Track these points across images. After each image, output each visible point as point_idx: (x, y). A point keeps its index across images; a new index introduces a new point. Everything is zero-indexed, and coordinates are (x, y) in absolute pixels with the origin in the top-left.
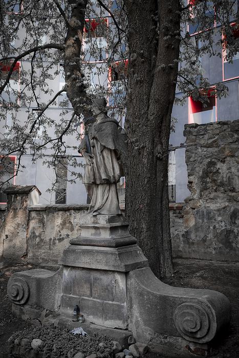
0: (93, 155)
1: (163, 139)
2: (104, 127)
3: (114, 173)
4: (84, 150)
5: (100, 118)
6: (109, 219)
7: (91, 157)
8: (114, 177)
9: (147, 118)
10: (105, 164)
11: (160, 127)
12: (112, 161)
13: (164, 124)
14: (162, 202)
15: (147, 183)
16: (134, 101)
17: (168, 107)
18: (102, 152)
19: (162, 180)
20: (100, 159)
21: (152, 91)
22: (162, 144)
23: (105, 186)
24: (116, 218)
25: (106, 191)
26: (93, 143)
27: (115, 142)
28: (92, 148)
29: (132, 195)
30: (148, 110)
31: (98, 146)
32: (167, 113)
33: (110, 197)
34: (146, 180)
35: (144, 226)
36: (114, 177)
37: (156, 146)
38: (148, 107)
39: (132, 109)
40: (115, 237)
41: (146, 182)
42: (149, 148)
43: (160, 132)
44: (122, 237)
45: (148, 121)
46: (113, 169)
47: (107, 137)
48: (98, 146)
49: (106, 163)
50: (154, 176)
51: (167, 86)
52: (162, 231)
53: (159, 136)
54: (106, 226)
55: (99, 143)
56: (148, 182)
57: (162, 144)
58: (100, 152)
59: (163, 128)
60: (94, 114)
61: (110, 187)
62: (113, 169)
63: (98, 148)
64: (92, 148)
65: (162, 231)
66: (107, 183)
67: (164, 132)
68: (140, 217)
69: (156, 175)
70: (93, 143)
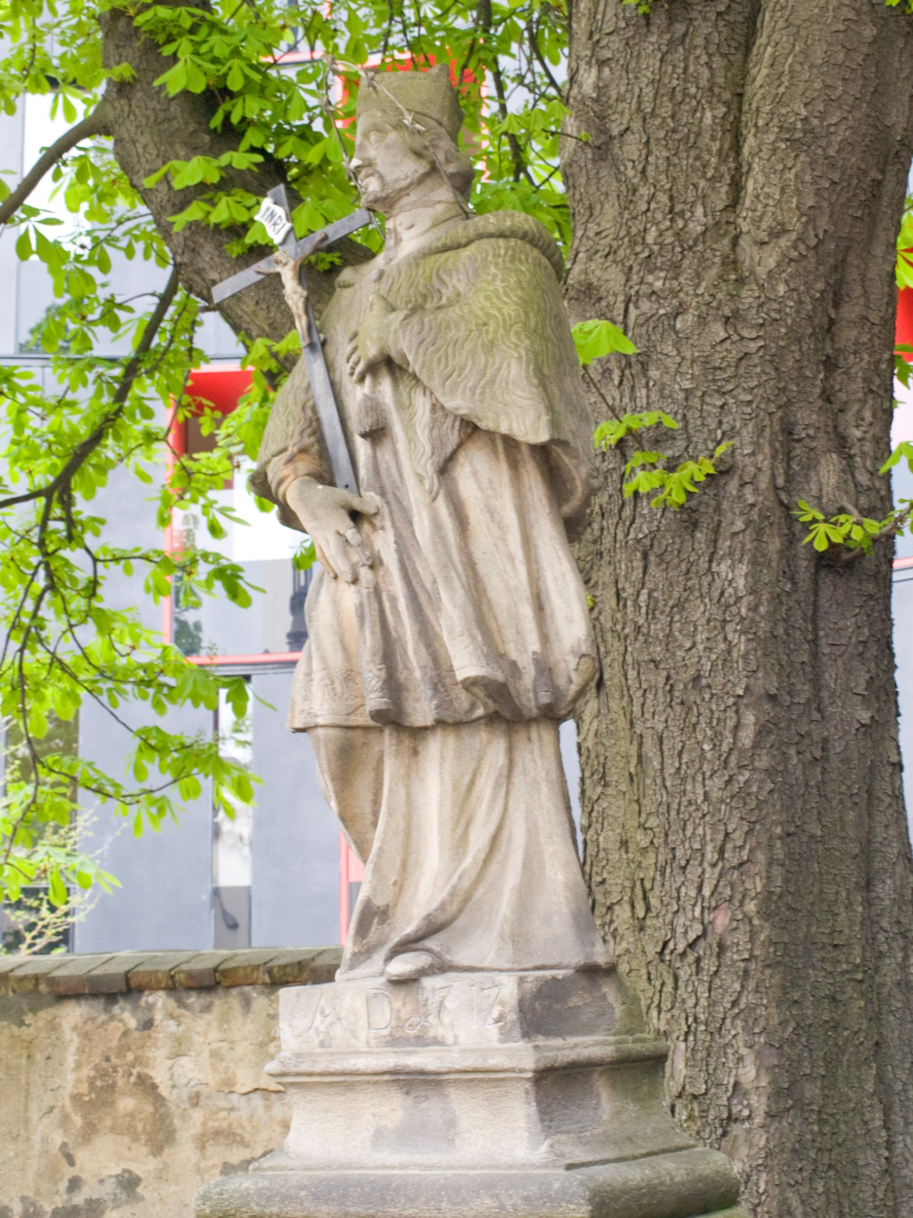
0: (370, 501)
1: (850, 416)
2: (457, 283)
3: (545, 638)
4: (304, 465)
5: (425, 216)
6: (521, 1002)
7: (356, 516)
8: (545, 668)
9: (731, 263)
10: (471, 565)
11: (830, 328)
12: (527, 541)
13: (850, 311)
14: (868, 885)
15: (756, 745)
16: (632, 149)
17: (878, 183)
18: (445, 469)
19: (865, 716)
20: (437, 525)
21: (760, 73)
22: (842, 443)
23: (483, 735)
24: (574, 1001)
25: (485, 786)
26: (373, 406)
27: (554, 389)
28: (362, 447)
29: (642, 840)
30: (734, 203)
31: (409, 427)
32: (874, 223)
33: (517, 831)
34: (749, 718)
35: (748, 1073)
36: (545, 668)
37: (810, 466)
38: (737, 187)
39: (610, 210)
40: (580, 1155)
41: (747, 737)
42: (764, 482)
43: (830, 365)
44: (628, 1151)
45: (741, 281)
46: (540, 605)
47: (490, 347)
48: (409, 427)
49: (478, 555)
50: (805, 691)
51: (869, 32)
52: (887, 1111)
53: (827, 397)
54: (494, 1062)
55: (422, 405)
56: (762, 732)
57: (842, 443)
58: (429, 470)
59: (848, 335)
60: (372, 186)
61: (510, 750)
62: (540, 605)
63: (411, 440)
64: (362, 447)
65: (887, 1111)
66: (492, 719)
67: (858, 364)
68: (712, 1004)
69: (816, 683)
70: (373, 406)
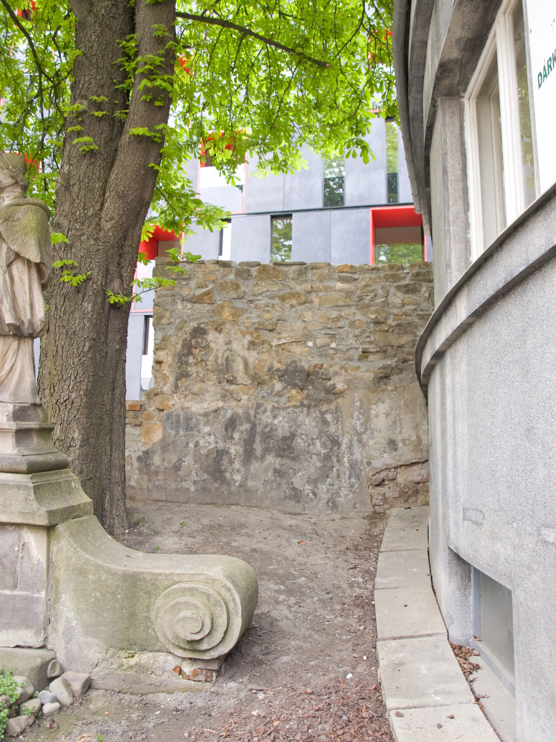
1: (124, 270)
3: (32, 315)
5: (12, 195)
6: (14, 411)
8: (31, 323)
9: (98, 224)
10: (13, 293)
12: (30, 289)
13: (128, 243)
14: (113, 390)
15: (88, 351)
16: (75, 189)
17: (139, 212)
18: (9, 265)
19: (118, 347)
21: (113, 176)
22: (121, 277)
23: (11, 340)
24: (29, 412)
25: (11, 353)
27: (43, 249)
29: (55, 372)
30: (101, 209)
32: (137, 221)
33: (18, 366)
34: (87, 344)
35: (76, 435)
36: (31, 323)
37: (112, 281)
38: (102, 205)
40: (26, 453)
41: (86, 349)
42: (99, 283)
43: (121, 256)
44: (40, 452)
45: (100, 230)
47: (26, 234)
49: (16, 290)
50: (103, 339)
52: (111, 447)
53: (119, 264)
54: (4, 427)
56: (90, 348)
57: (121, 277)
59: (126, 249)
61: (19, 344)
65: (111, 447)
66: (15, 335)
67: (128, 257)
68: (69, 417)
69: (106, 337)
